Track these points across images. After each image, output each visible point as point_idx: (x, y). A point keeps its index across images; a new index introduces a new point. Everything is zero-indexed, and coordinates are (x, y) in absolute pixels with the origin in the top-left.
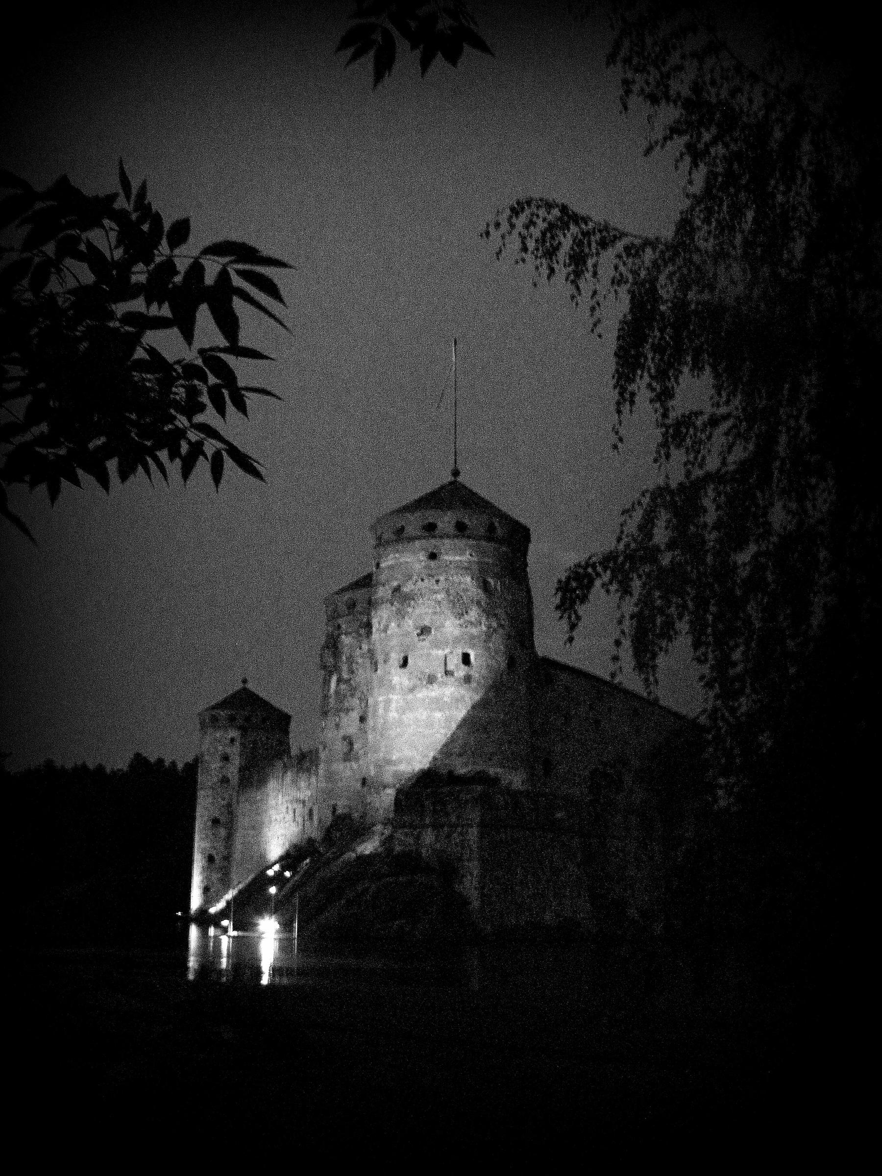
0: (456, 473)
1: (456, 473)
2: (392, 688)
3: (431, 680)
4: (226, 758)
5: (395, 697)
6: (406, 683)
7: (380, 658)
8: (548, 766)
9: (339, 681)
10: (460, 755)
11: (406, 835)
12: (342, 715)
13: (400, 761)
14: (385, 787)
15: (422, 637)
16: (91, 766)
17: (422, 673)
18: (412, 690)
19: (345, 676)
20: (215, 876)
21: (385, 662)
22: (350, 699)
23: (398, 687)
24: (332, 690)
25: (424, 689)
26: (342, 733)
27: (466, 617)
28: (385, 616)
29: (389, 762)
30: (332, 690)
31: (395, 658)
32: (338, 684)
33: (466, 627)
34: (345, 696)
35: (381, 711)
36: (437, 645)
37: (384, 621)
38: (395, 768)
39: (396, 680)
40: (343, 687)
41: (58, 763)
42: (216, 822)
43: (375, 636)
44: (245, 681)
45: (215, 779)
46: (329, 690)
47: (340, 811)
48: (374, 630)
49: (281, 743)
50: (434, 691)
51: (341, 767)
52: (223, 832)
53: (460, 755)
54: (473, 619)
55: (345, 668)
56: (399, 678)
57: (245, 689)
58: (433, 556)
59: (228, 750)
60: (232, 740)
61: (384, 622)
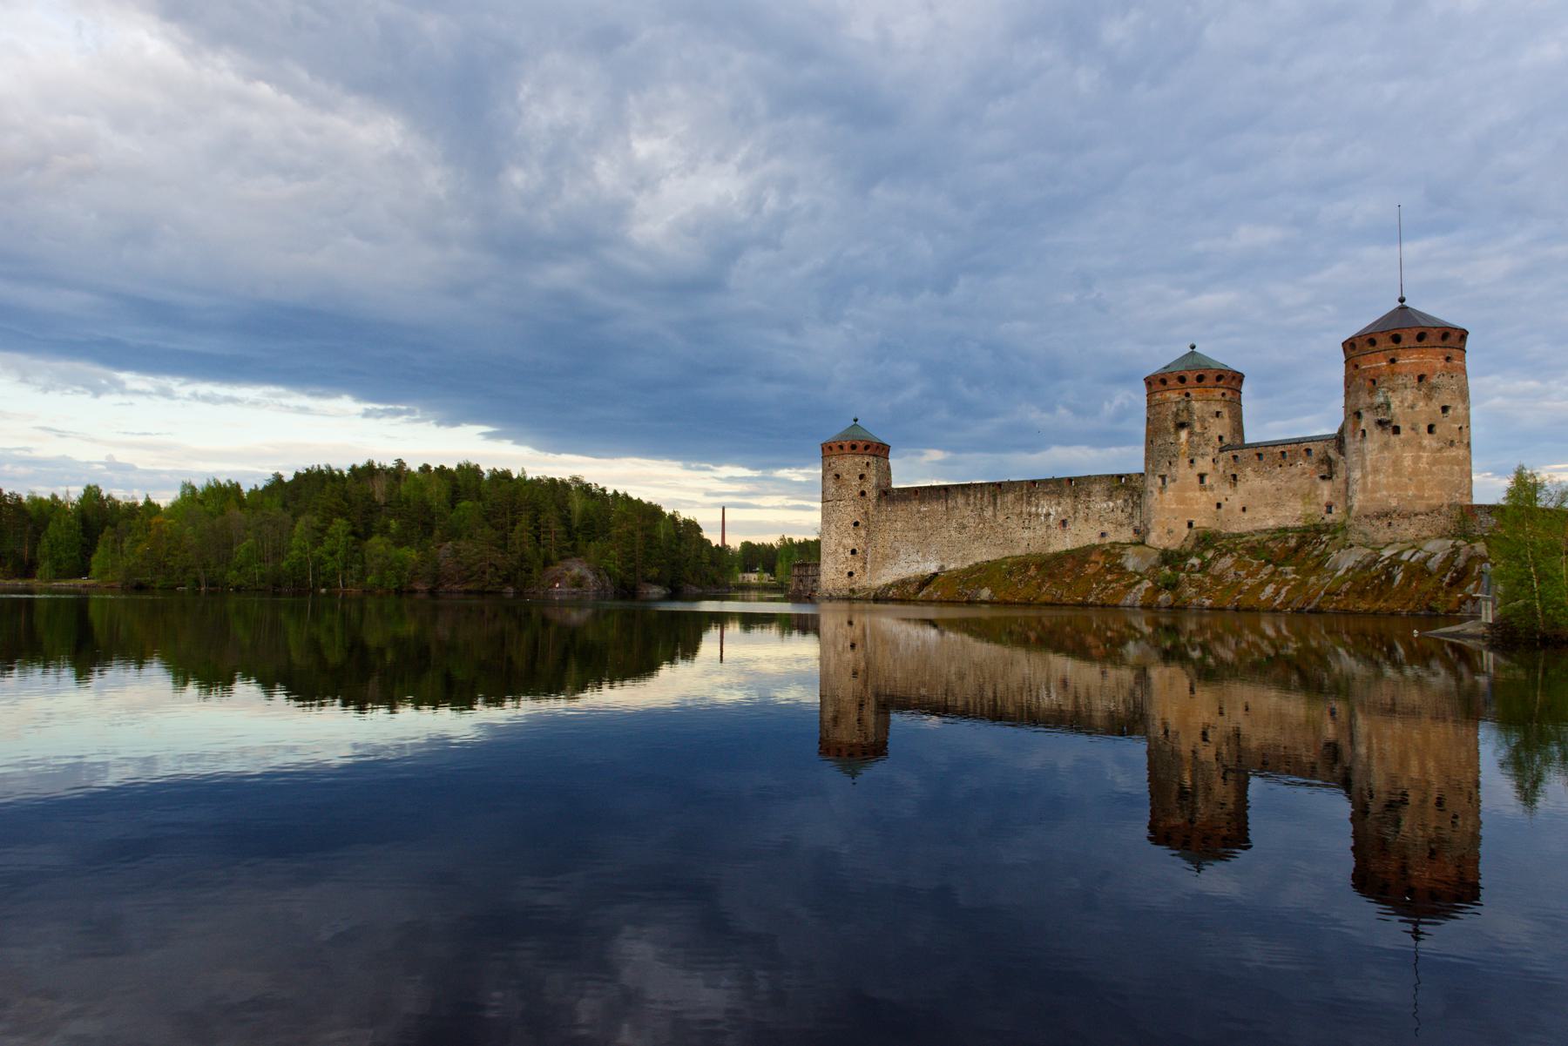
0: (1402, 300)
1: (1402, 300)
2: (1421, 447)
3: (1452, 443)
4: (861, 477)
6: (1435, 445)
9: (1191, 434)
13: (1431, 498)
19: (1197, 429)
20: (858, 565)
26: (1197, 471)
28: (1410, 398)
29: (1422, 498)
31: (1423, 428)
35: (1407, 462)
36: (1454, 420)
39: (1425, 442)
40: (1196, 439)
42: (856, 524)
51: (1198, 494)
52: (863, 533)
56: (1427, 440)
58: (1448, 359)
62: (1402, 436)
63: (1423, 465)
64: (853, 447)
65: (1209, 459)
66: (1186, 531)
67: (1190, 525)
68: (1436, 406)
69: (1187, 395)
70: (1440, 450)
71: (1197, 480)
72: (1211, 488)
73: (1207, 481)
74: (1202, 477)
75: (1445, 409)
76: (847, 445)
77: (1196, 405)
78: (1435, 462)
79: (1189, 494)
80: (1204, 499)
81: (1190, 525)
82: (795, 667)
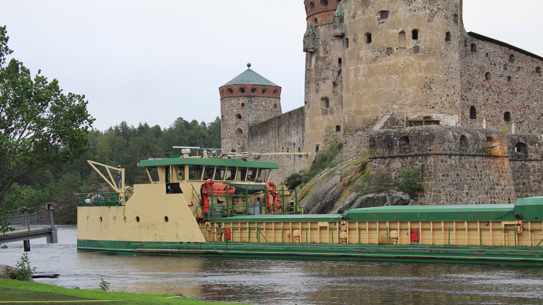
2: (359, 59)
3: (389, 51)
4: (239, 117)
5: (361, 66)
6: (370, 55)
7: (350, 37)
8: (473, 113)
9: (317, 59)
10: (411, 105)
11: (379, 163)
12: (321, 83)
14: (356, 131)
15: (381, 21)
16: (151, 126)
17: (382, 47)
18: (375, 60)
19: (321, 54)
21: (354, 40)
22: (326, 71)
23: (364, 58)
24: (313, 66)
25: (384, 59)
26: (321, 95)
27: (414, 4)
28: (353, 7)
29: (359, 112)
30: (313, 66)
31: (362, 38)
32: (316, 63)
33: (415, 11)
34: (322, 69)
35: (352, 77)
36: (393, 26)
37: (352, 10)
38: (364, 117)
39: (362, 53)
40: (320, 63)
41: (129, 125)
43: (346, 21)
44: (249, 65)
45: (233, 131)
46: (310, 66)
47: (320, 149)
48: (345, 18)
49: (275, 106)
50: (391, 60)
51: (321, 118)
53: (411, 105)
54: (420, 6)
55: (321, 49)
56: (365, 51)
57: (249, 70)
59: (241, 112)
60: (243, 104)
61: (352, 12)
62: (350, 48)
63: (361, 78)
64: (242, 90)
65: (330, 82)
66: (315, 154)
67: (317, 148)
68: (372, 13)
69: (316, 20)
70: (375, 60)
71: (320, 105)
72: (332, 113)
73: (331, 104)
74: (326, 100)
75: (384, 14)
76: (236, 89)
77: (321, 29)
78: (371, 73)
79: (316, 119)
80: (326, 123)
81: (317, 148)
82: (88, 288)
